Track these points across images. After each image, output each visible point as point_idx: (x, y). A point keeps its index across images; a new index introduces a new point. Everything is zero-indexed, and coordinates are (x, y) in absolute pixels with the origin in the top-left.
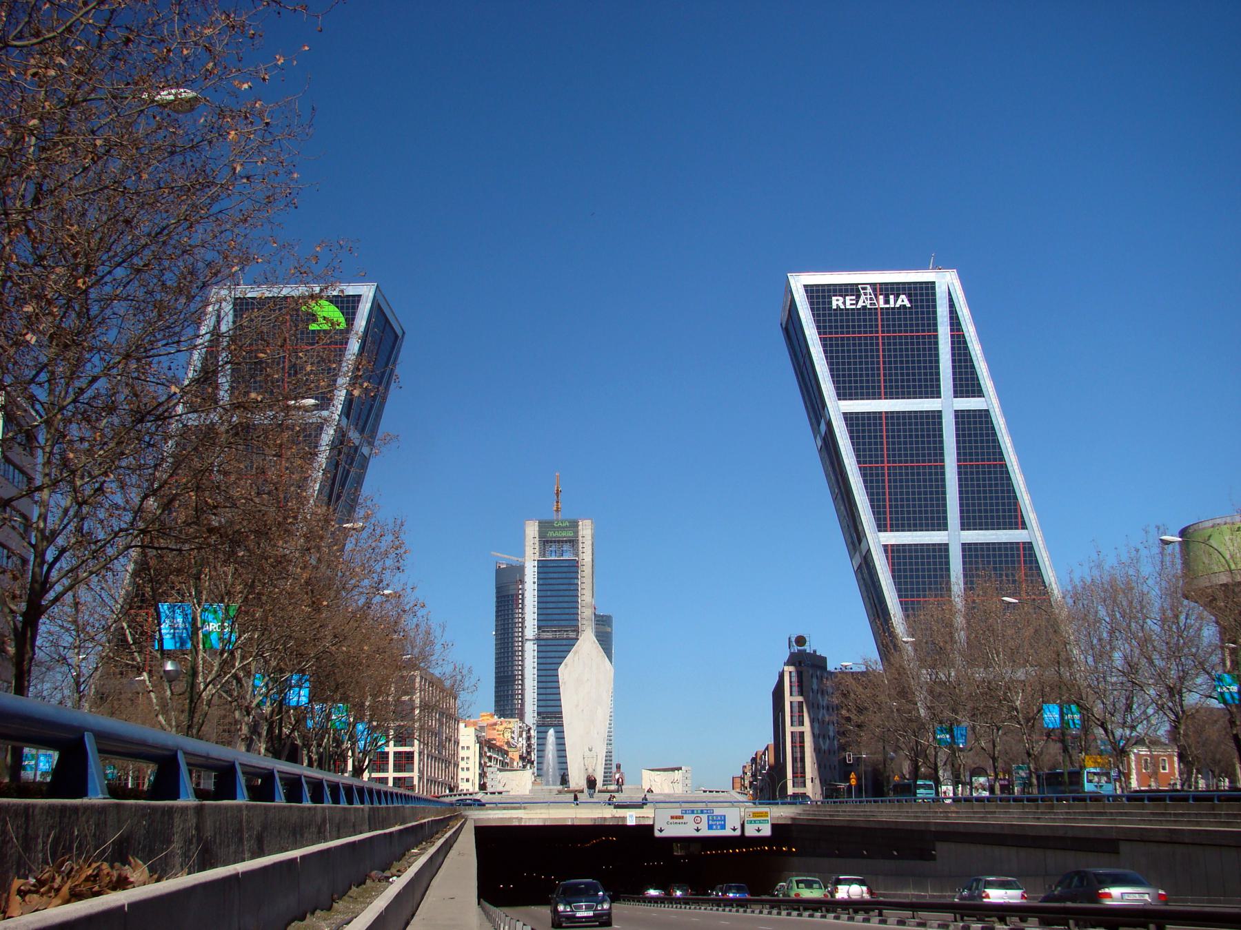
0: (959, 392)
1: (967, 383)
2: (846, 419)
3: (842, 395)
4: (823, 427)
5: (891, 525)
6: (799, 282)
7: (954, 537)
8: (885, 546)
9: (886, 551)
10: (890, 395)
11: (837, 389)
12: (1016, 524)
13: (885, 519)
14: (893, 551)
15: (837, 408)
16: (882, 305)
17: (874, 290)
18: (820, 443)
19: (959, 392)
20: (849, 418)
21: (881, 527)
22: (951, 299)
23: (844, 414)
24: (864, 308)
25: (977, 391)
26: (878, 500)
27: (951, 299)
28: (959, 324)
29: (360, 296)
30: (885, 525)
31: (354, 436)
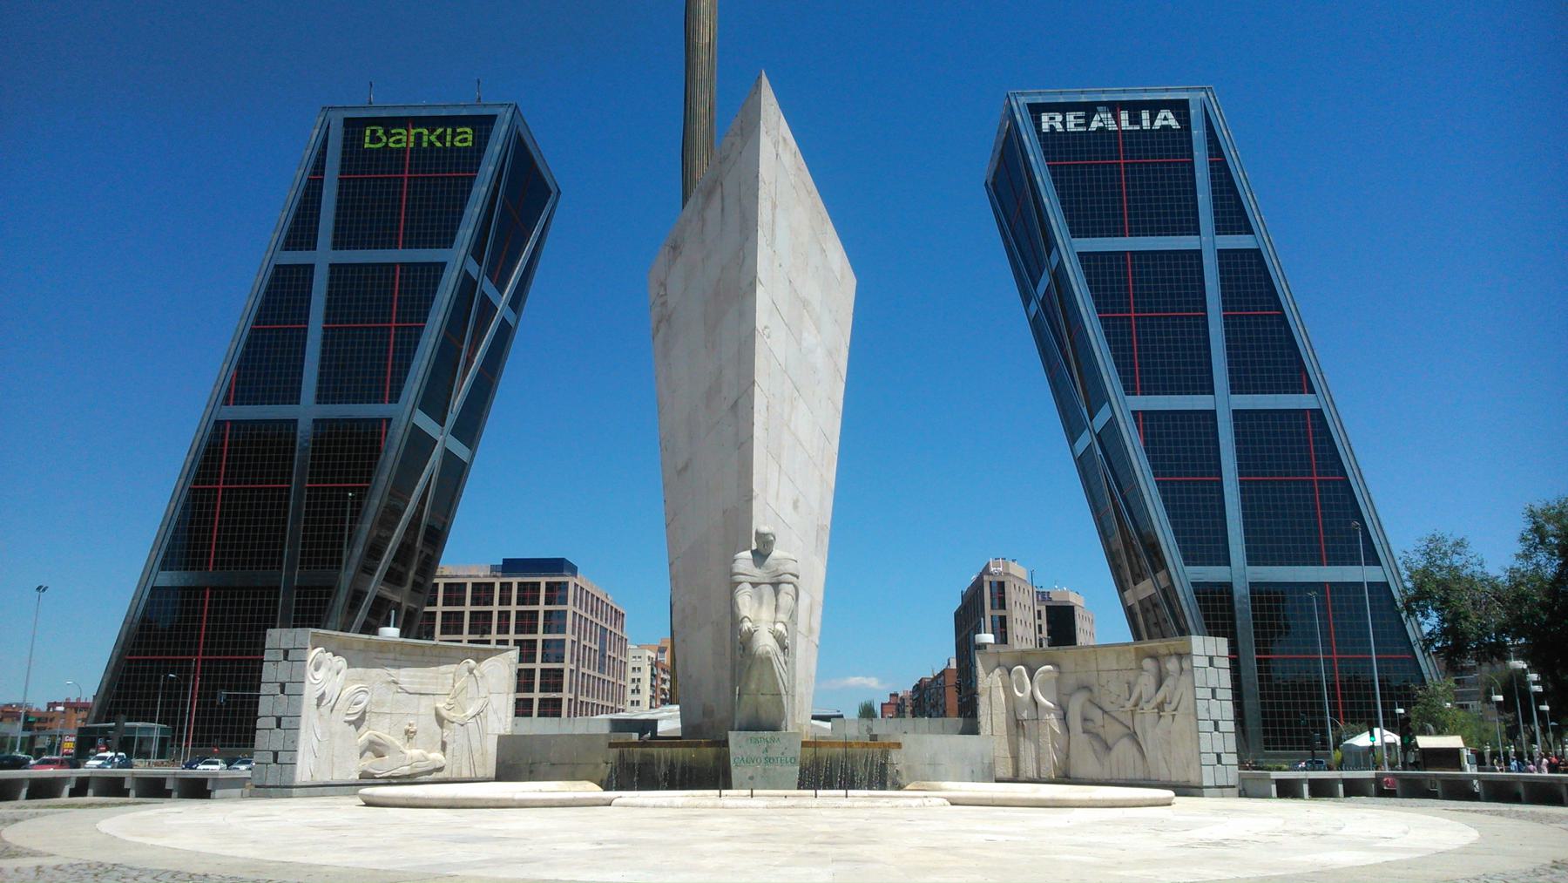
0: (1222, 228)
1: (1232, 216)
2: (1081, 260)
3: (1076, 232)
4: (1045, 280)
7: (1223, 402)
9: (1136, 419)
10: (1136, 232)
11: (1070, 224)
12: (1301, 386)
13: (1134, 380)
15: (1070, 248)
16: (1125, 125)
18: (1033, 307)
19: (1222, 228)
20: (1083, 257)
21: (1129, 389)
26: (1124, 357)
28: (1220, 152)
29: (495, 117)
30: (1134, 388)
31: (487, 287)
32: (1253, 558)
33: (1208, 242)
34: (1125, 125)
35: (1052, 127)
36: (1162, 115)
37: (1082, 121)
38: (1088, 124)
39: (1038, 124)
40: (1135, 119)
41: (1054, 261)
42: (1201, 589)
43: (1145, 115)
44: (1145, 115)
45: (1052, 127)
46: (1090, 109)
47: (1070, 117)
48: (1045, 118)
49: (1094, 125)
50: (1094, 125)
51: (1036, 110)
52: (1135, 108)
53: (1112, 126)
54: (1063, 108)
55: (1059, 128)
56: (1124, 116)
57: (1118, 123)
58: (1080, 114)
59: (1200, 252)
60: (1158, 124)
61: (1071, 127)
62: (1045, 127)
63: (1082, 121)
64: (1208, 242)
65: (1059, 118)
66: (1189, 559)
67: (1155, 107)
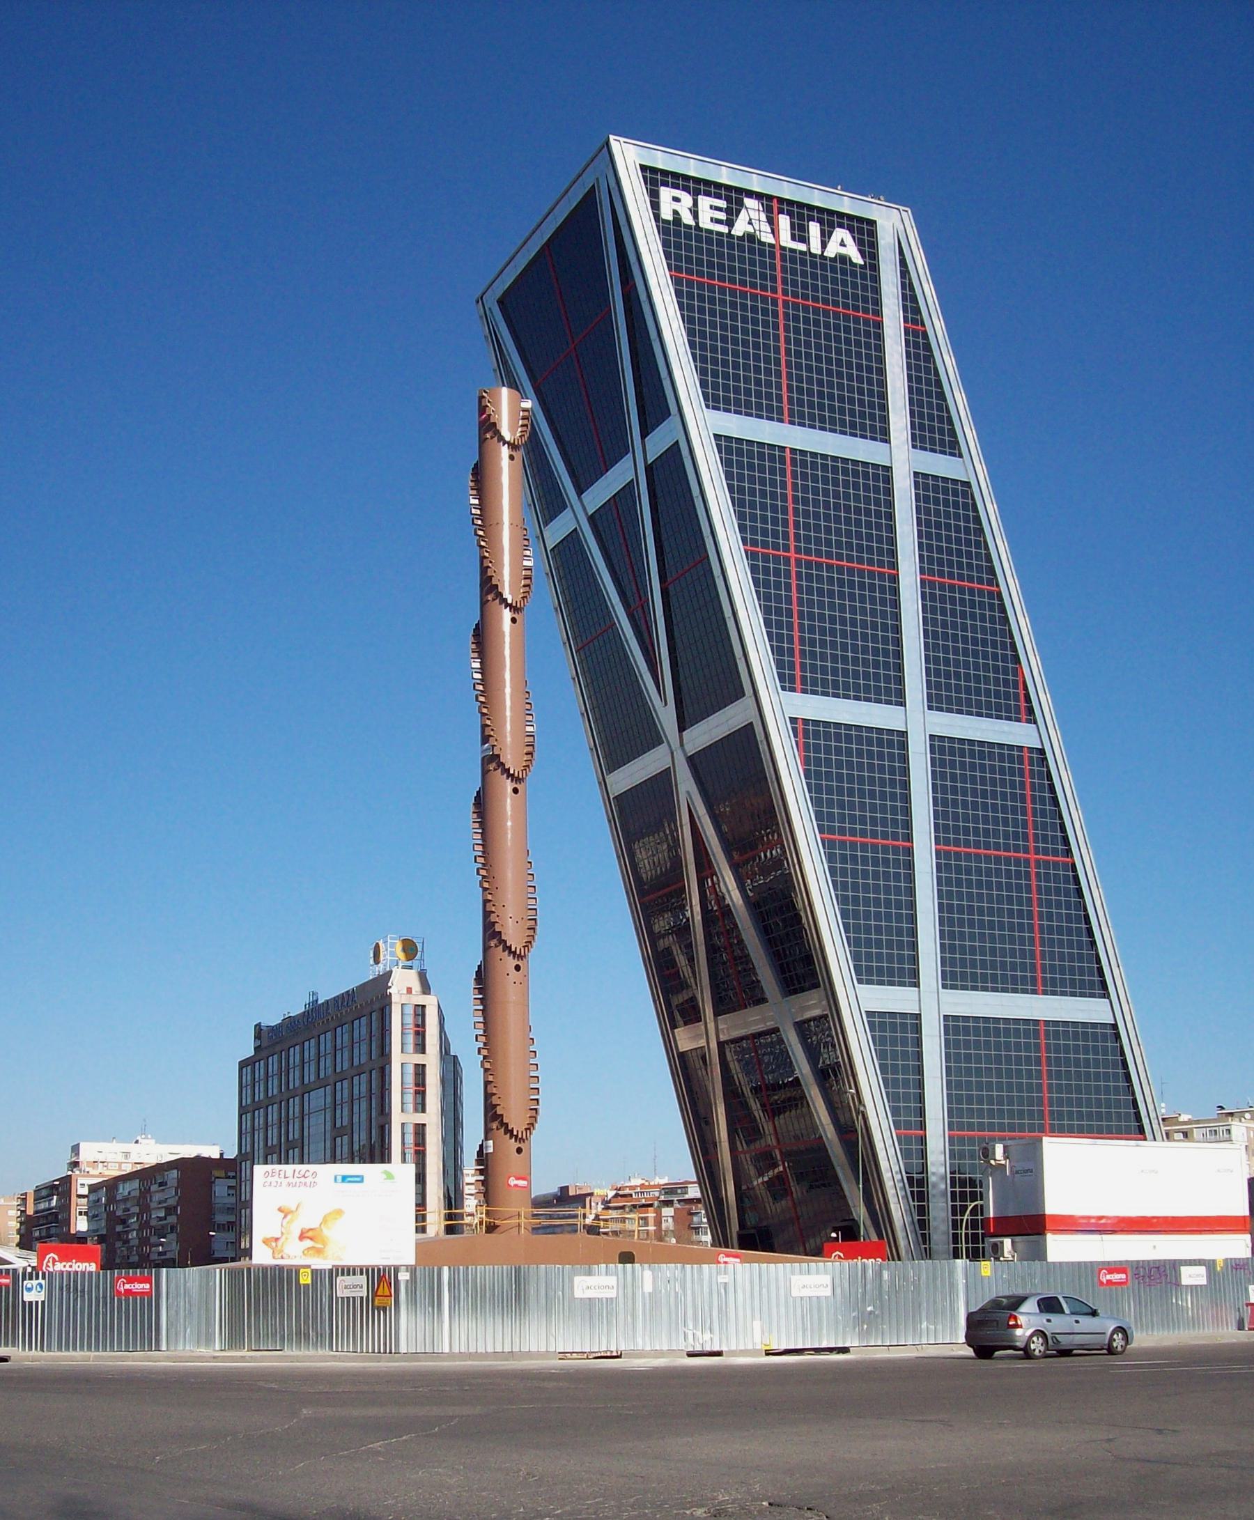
3: (714, 400)
5: (804, 680)
6: (629, 156)
8: (793, 720)
10: (799, 419)
14: (806, 732)
15: (703, 425)
16: (786, 240)
17: (768, 210)
20: (726, 445)
22: (903, 262)
23: (717, 437)
24: (751, 238)
25: (951, 446)
27: (903, 262)
28: (917, 311)
30: (792, 679)
32: (952, 978)
33: (902, 457)
34: (786, 240)
35: (675, 212)
36: (840, 234)
37: (722, 216)
38: (730, 223)
39: (655, 206)
40: (800, 233)
41: (658, 443)
42: (879, 1022)
43: (814, 229)
44: (814, 229)
45: (675, 212)
46: (734, 198)
47: (705, 202)
48: (666, 194)
49: (740, 228)
50: (740, 228)
51: (654, 178)
52: (801, 214)
53: (768, 238)
54: (697, 186)
55: (687, 219)
56: (784, 222)
57: (774, 232)
58: (722, 204)
59: (888, 469)
60: (832, 250)
61: (705, 223)
62: (666, 214)
63: (722, 216)
64: (902, 457)
65: (687, 199)
66: (867, 973)
67: (831, 220)
